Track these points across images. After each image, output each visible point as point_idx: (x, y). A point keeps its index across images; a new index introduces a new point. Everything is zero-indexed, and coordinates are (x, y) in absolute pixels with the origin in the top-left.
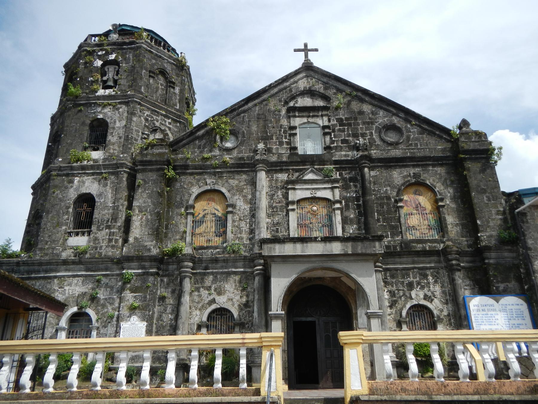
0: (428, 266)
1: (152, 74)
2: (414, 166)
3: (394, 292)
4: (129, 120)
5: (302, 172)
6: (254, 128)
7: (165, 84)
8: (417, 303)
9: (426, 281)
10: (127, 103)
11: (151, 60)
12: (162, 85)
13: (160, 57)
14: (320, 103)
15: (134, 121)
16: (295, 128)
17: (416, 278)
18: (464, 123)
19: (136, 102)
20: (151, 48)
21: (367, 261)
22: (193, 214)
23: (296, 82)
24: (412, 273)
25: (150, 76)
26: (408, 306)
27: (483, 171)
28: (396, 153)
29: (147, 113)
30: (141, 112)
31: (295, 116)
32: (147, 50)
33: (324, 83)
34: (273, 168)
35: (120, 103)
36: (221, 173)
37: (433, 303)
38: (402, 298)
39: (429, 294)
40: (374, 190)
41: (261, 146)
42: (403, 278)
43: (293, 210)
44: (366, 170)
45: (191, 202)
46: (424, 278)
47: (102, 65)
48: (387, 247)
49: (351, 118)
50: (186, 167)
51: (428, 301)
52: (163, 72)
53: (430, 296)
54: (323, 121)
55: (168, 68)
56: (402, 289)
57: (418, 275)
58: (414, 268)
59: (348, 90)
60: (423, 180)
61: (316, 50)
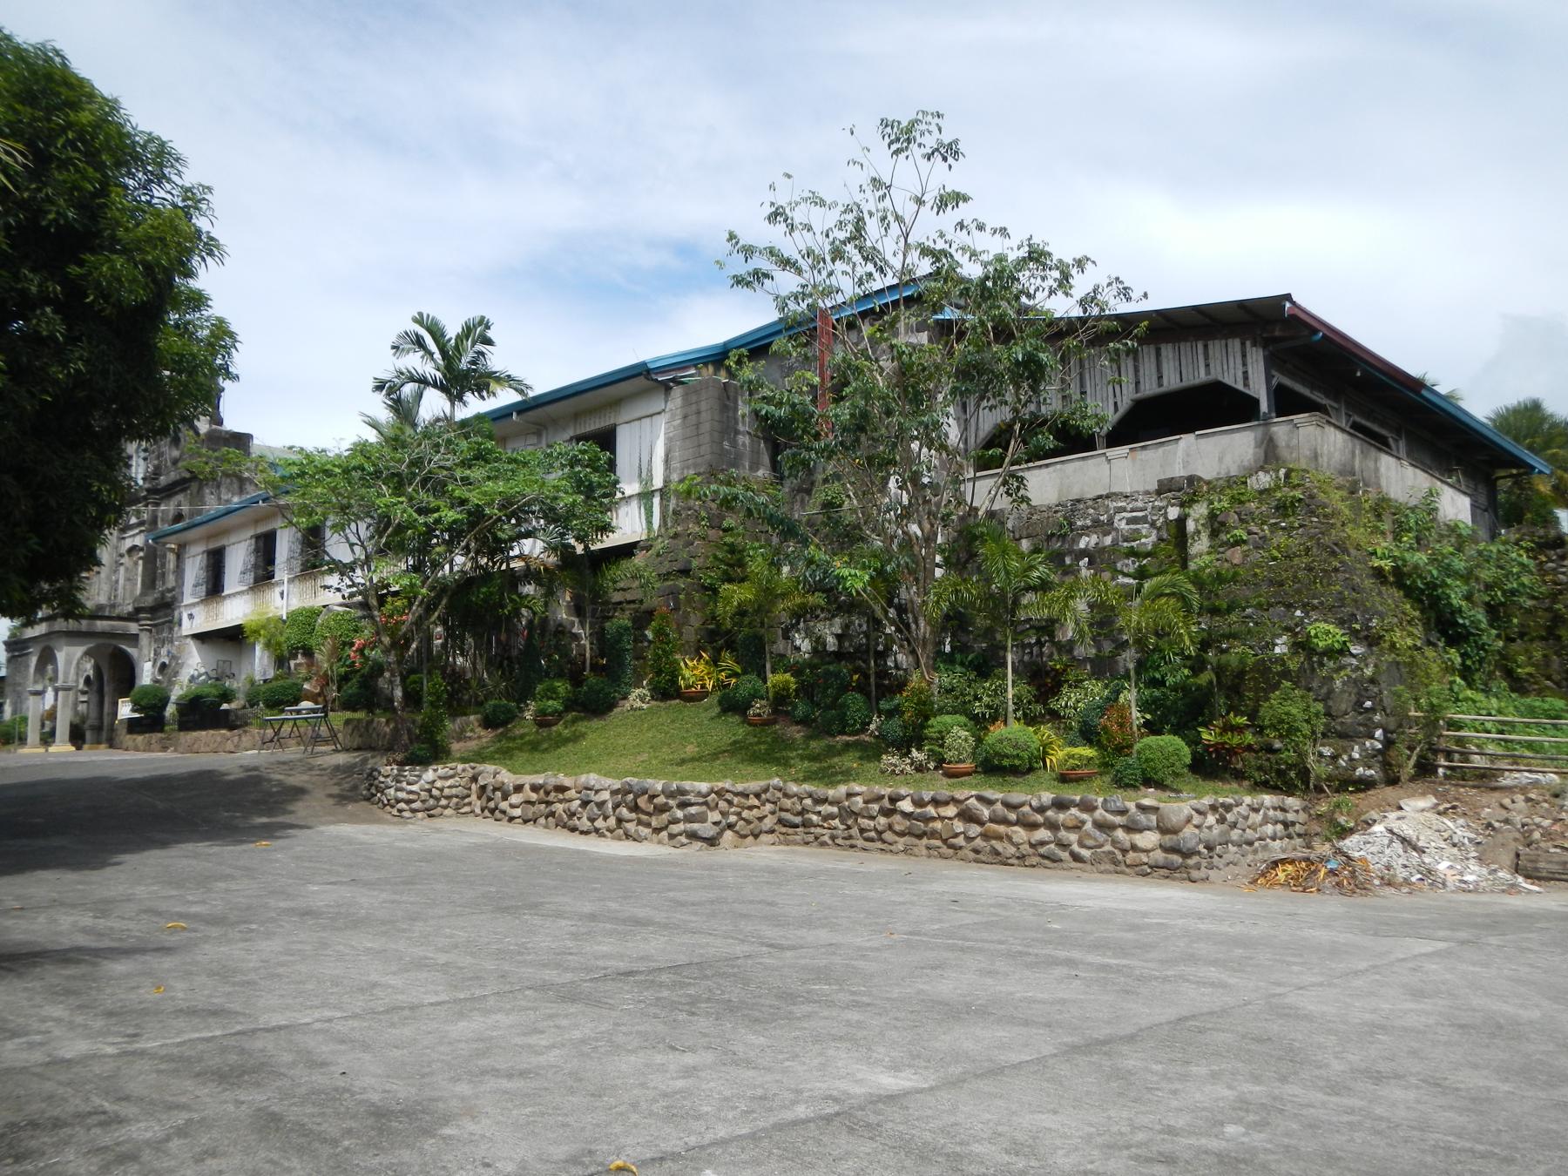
28: (173, 476)
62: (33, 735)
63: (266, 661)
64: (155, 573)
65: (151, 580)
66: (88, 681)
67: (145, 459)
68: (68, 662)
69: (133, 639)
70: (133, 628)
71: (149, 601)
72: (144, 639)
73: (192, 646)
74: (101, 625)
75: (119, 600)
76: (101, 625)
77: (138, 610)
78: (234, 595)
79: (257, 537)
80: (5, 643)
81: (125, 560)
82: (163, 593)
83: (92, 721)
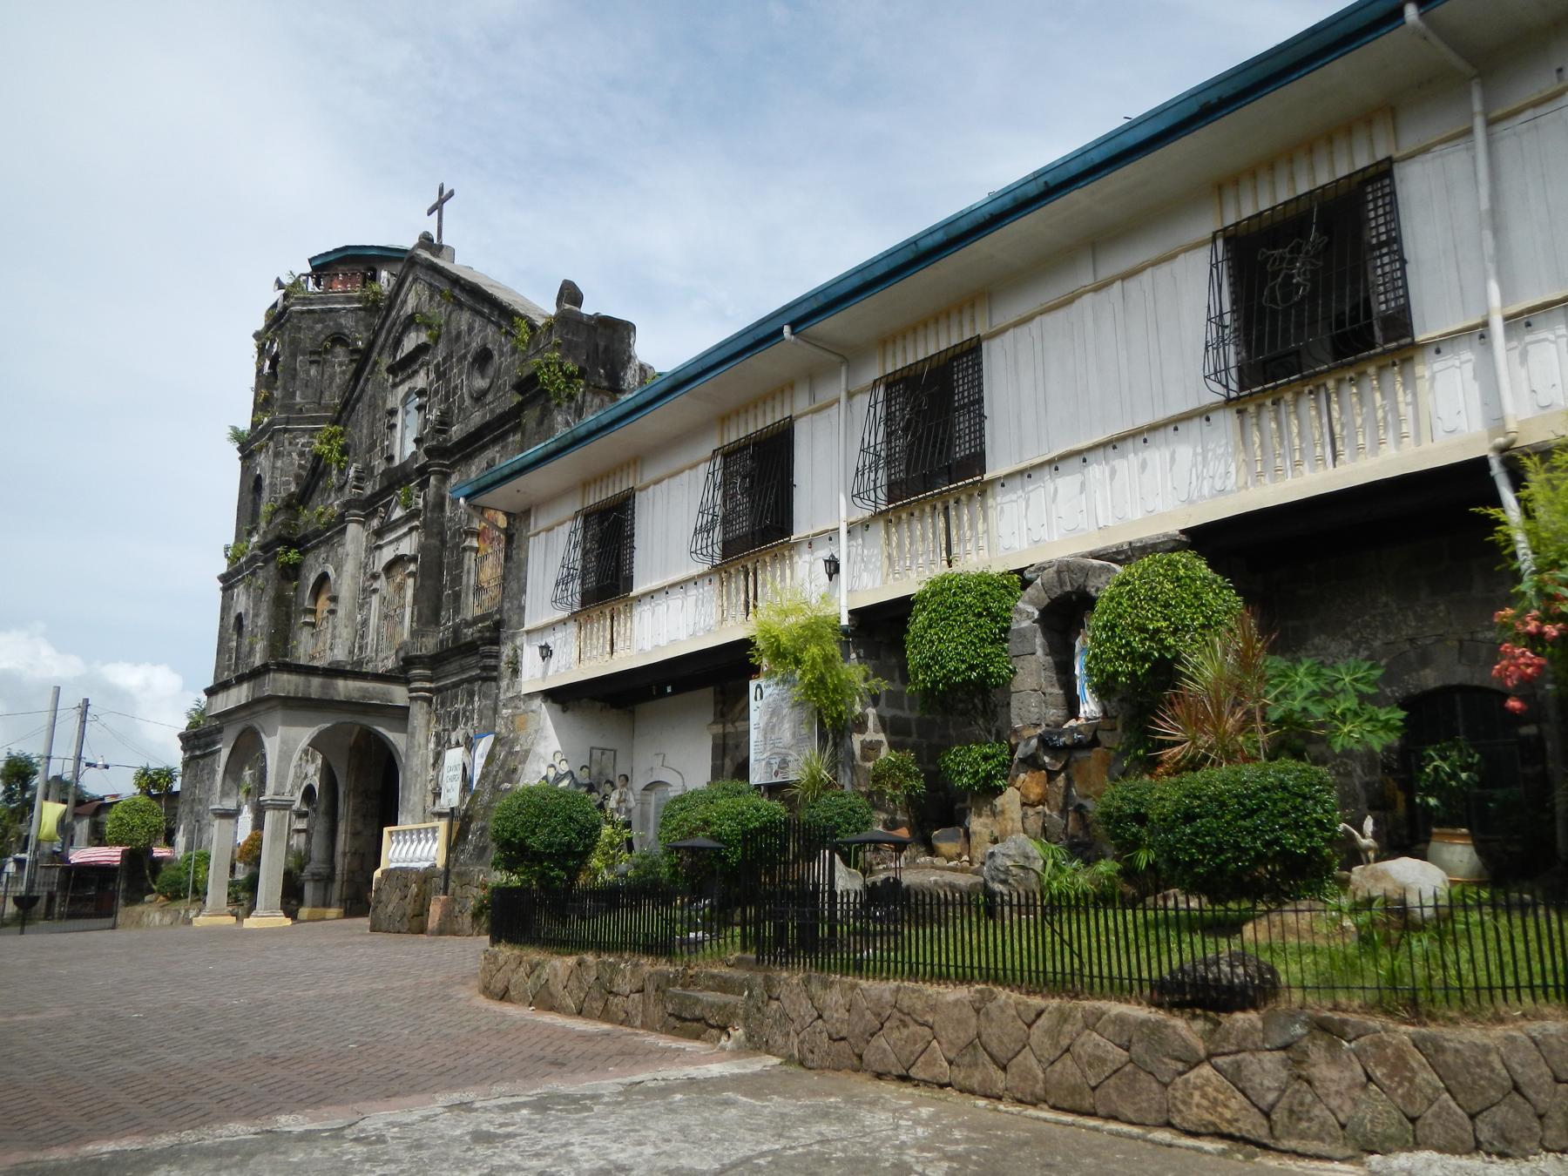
1: (319, 355)
2: (494, 441)
4: (274, 467)
5: (387, 506)
7: (347, 360)
10: (270, 438)
11: (311, 328)
12: (341, 364)
13: (331, 310)
14: (423, 337)
16: (393, 413)
18: (570, 294)
21: (273, 708)
22: (313, 625)
23: (404, 302)
25: (312, 362)
27: (540, 423)
28: (477, 418)
29: (303, 440)
32: (302, 312)
33: (431, 285)
34: (368, 507)
36: (331, 537)
40: (451, 519)
41: (352, 472)
43: (375, 591)
44: (432, 480)
45: (307, 604)
47: (273, 366)
48: (442, 642)
50: (306, 538)
52: (338, 339)
54: (420, 381)
55: (348, 323)
58: (462, 682)
59: (446, 288)
61: (451, 194)
62: (217, 891)
63: (786, 732)
65: (431, 607)
66: (309, 793)
67: (420, 408)
68: (285, 757)
69: (400, 716)
70: (399, 695)
71: (429, 645)
72: (419, 715)
73: (545, 716)
74: (345, 688)
75: (369, 653)
76: (345, 688)
77: (409, 662)
78: (651, 594)
79: (729, 454)
80: (181, 736)
82: (456, 630)
83: (316, 865)
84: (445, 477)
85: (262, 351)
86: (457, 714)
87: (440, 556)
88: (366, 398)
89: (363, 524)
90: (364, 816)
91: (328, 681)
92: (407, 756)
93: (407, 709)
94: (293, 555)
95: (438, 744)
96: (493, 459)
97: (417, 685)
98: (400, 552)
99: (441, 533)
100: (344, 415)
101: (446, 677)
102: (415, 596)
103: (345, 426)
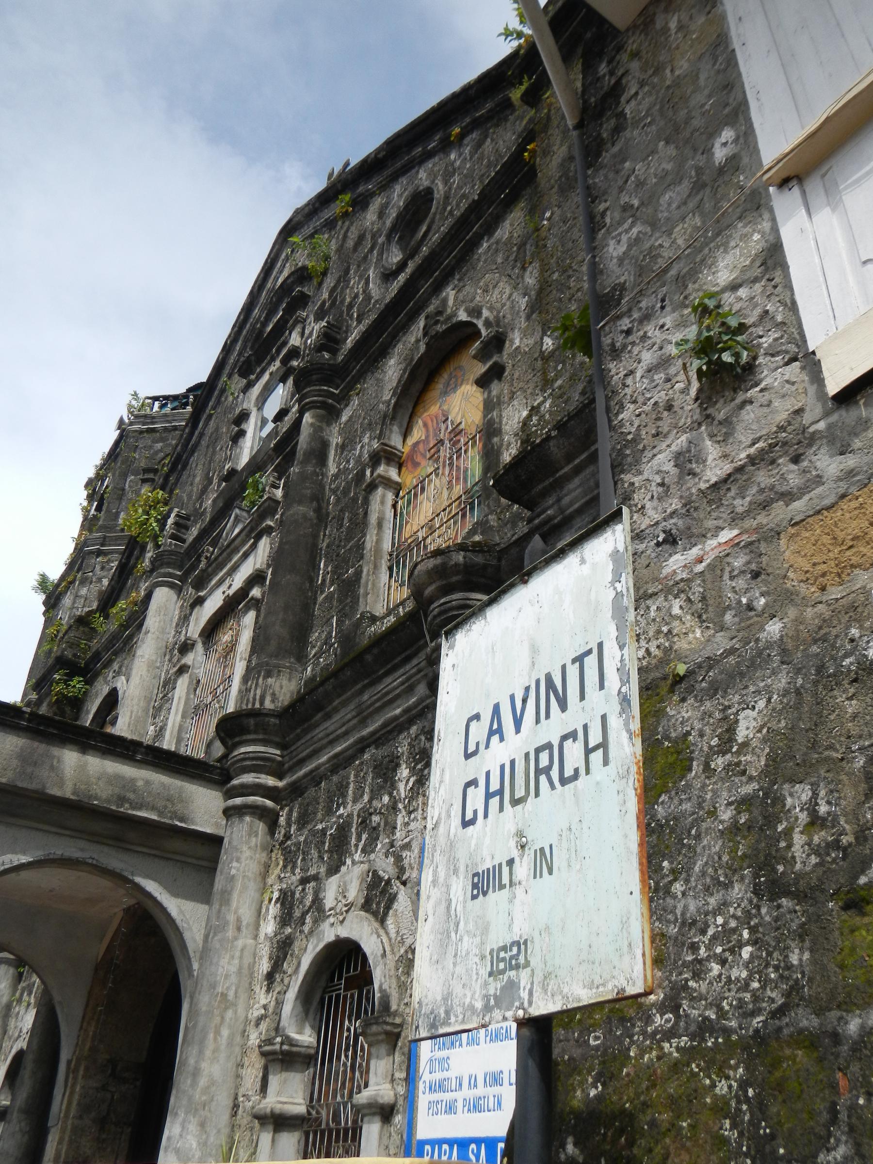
0: (398, 711)
3: (293, 893)
6: (198, 479)
8: (332, 938)
9: (386, 799)
11: (148, 448)
15: (81, 597)
17: (362, 796)
19: (91, 552)
20: (153, 423)
24: (356, 776)
25: (144, 481)
26: (306, 962)
30: (103, 568)
31: (250, 385)
32: (141, 432)
35: (78, 572)
37: (390, 921)
38: (308, 919)
39: (386, 867)
42: (329, 812)
43: (183, 670)
46: (385, 781)
49: (340, 277)
50: (97, 656)
51: (375, 914)
53: (388, 882)
56: (312, 872)
57: (369, 779)
58: (362, 746)
60: (450, 318)
64: (307, 608)
70: (203, 807)
72: (245, 851)
81: (196, 657)
84: (330, 413)
85: (90, 498)
86: (343, 830)
87: (315, 536)
88: (204, 443)
89: (179, 590)
90: (102, 1123)
91: (41, 747)
92: (205, 952)
93: (216, 841)
94: (77, 683)
95: (284, 919)
96: (445, 301)
97: (248, 778)
98: (231, 592)
99: (318, 498)
100: (172, 479)
101: (316, 753)
102: (255, 640)
103: (171, 492)
